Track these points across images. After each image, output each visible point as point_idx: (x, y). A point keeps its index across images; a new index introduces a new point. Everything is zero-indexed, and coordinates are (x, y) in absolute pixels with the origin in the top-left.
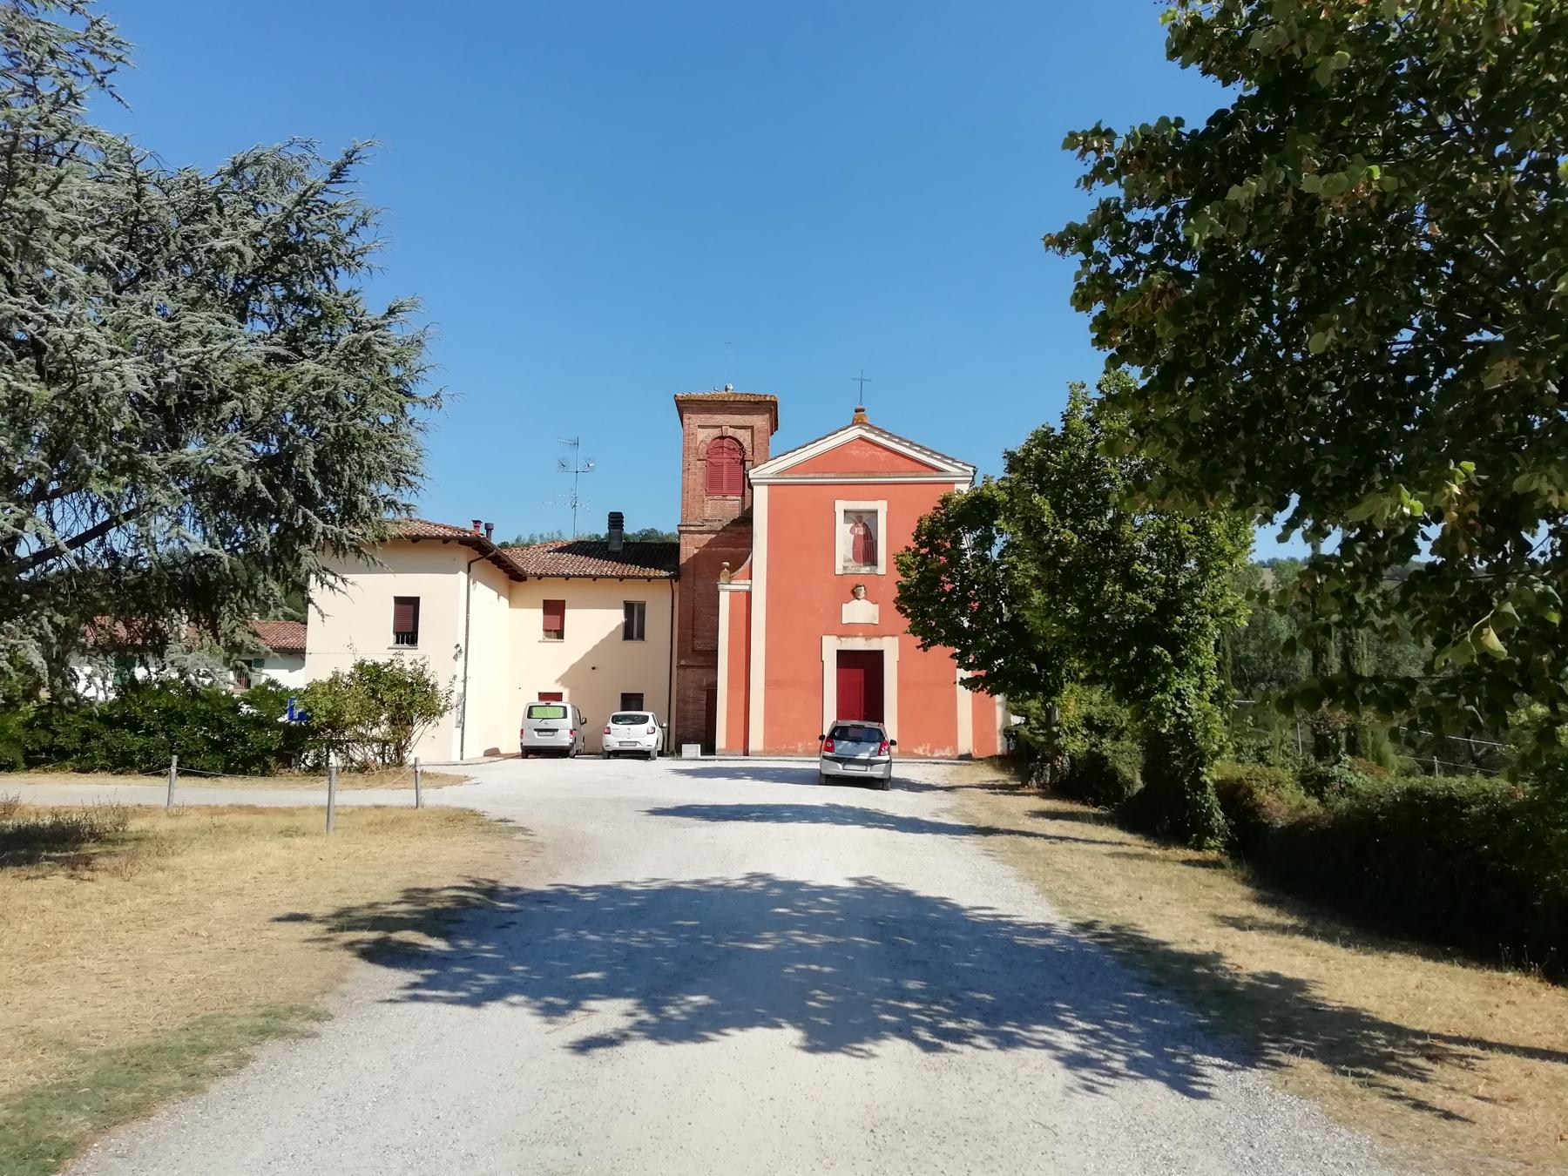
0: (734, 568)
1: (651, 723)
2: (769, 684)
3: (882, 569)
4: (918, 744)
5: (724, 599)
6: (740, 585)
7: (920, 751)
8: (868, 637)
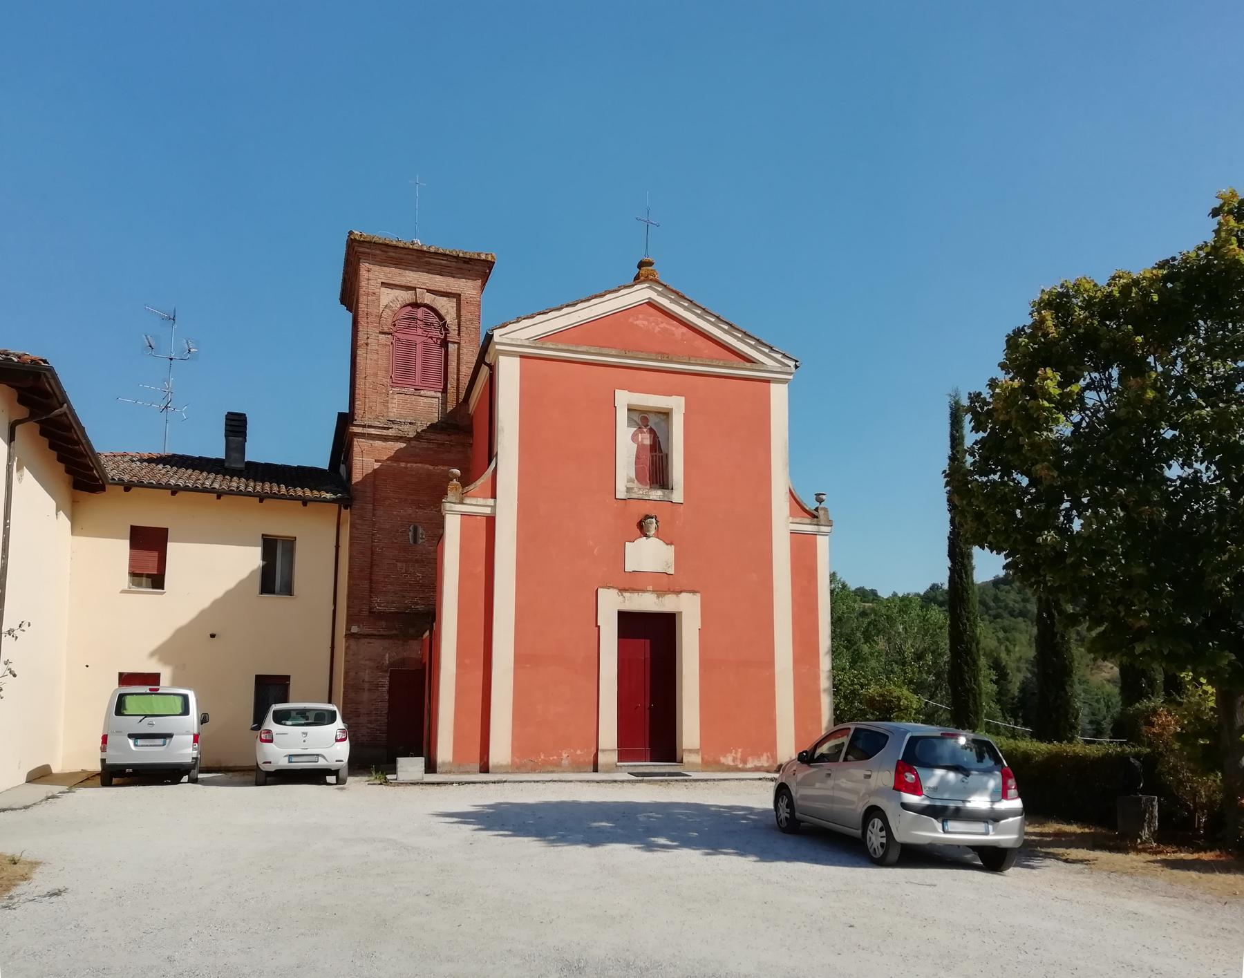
0: (466, 481)
1: (339, 724)
2: (521, 660)
3: (678, 496)
4: (725, 752)
5: (452, 526)
6: (477, 505)
7: (728, 760)
8: (660, 592)
